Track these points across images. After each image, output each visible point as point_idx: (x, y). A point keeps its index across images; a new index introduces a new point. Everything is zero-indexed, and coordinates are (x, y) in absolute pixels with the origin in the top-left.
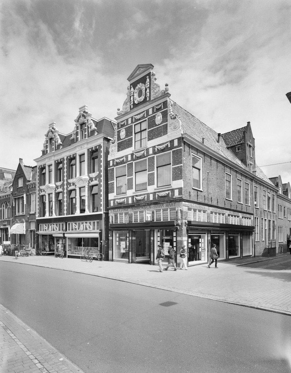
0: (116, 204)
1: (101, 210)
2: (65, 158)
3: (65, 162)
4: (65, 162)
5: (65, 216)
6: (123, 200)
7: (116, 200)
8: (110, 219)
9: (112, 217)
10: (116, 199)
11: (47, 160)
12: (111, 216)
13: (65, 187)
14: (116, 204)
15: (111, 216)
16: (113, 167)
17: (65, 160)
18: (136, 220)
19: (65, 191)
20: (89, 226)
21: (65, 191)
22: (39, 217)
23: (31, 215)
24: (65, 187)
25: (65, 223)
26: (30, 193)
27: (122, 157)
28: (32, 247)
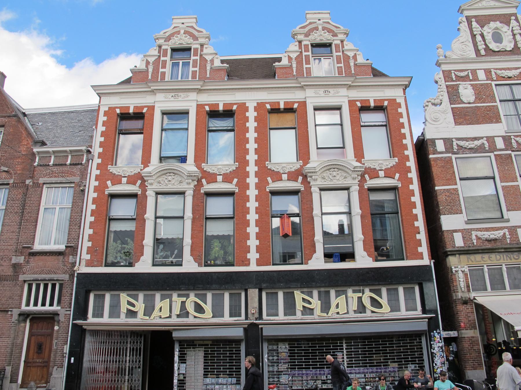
0: (475, 241)
1: (420, 256)
2: (251, 106)
3: (251, 114)
4: (251, 114)
5: (253, 267)
6: (501, 233)
7: (474, 233)
8: (462, 280)
9: (466, 275)
10: (474, 230)
11: (160, 97)
12: (460, 272)
13: (252, 180)
14: (475, 241)
15: (460, 272)
16: (450, 155)
17: (251, 109)
18: (409, 292)
19: (252, 192)
20: (372, 299)
21: (252, 192)
22: (89, 264)
23: (37, 258)
24: (252, 180)
25: (257, 290)
26: (41, 181)
27: (475, 139)
28: (16, 381)
